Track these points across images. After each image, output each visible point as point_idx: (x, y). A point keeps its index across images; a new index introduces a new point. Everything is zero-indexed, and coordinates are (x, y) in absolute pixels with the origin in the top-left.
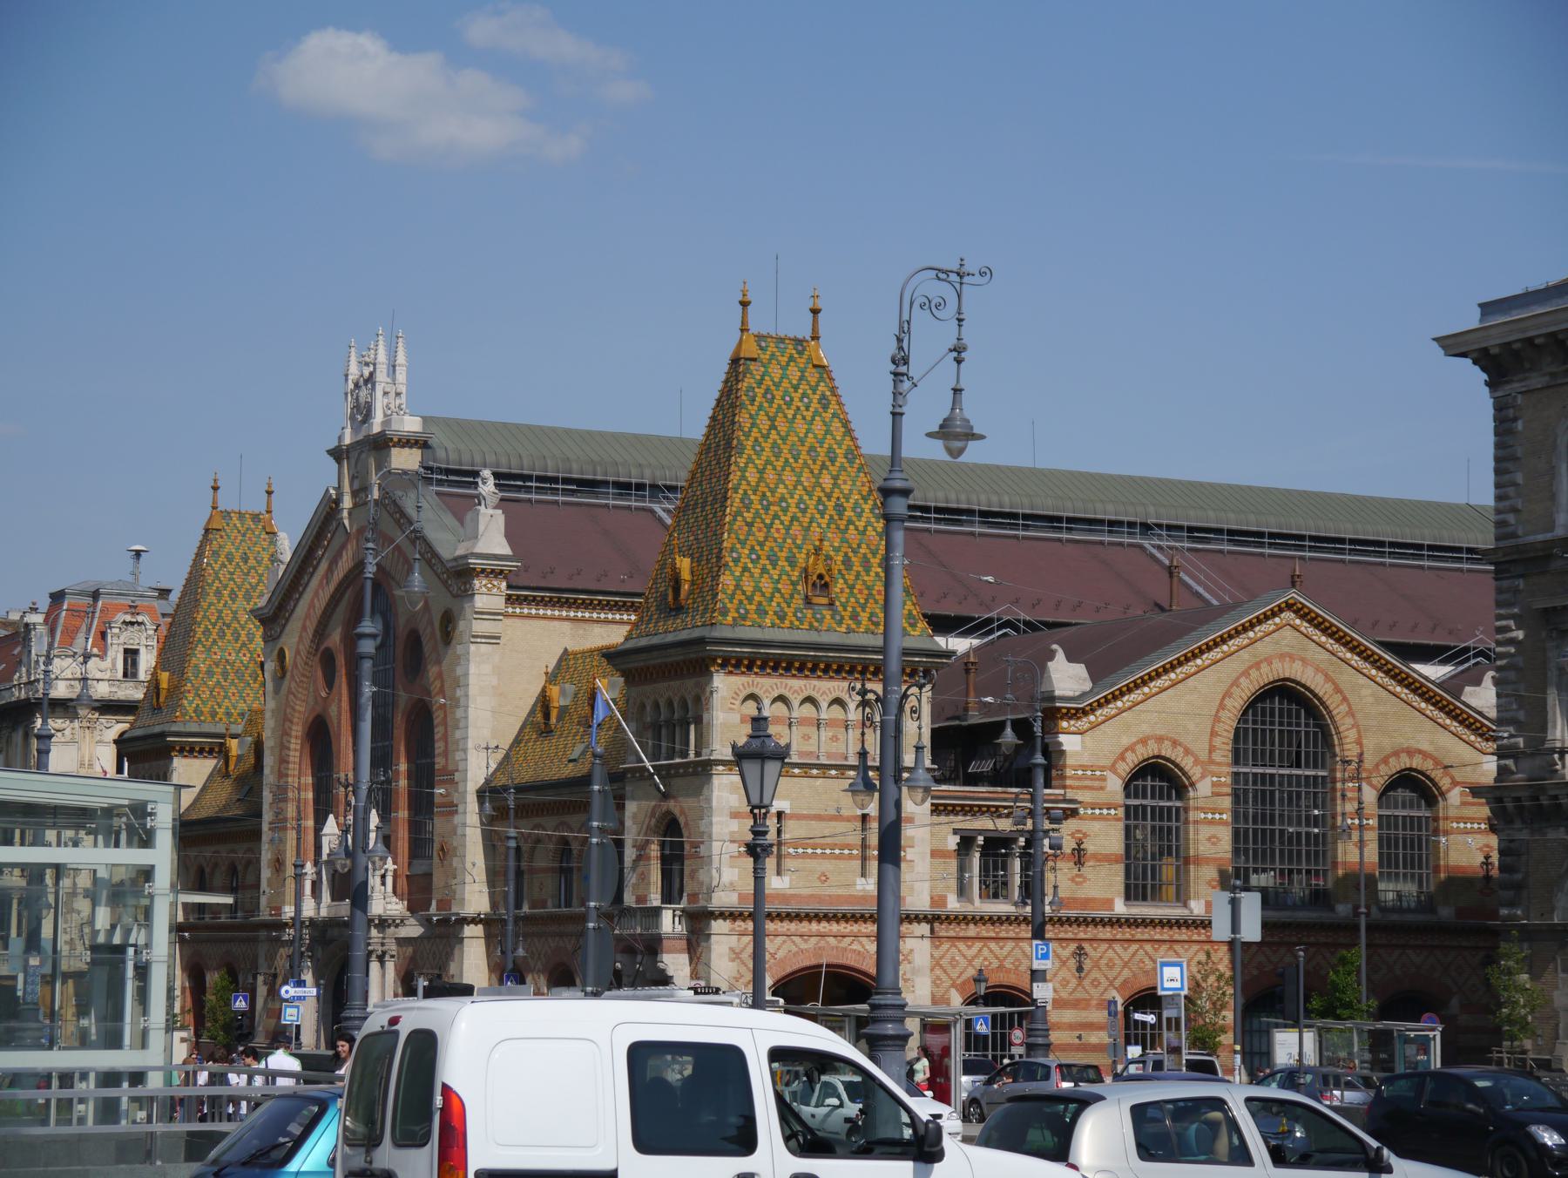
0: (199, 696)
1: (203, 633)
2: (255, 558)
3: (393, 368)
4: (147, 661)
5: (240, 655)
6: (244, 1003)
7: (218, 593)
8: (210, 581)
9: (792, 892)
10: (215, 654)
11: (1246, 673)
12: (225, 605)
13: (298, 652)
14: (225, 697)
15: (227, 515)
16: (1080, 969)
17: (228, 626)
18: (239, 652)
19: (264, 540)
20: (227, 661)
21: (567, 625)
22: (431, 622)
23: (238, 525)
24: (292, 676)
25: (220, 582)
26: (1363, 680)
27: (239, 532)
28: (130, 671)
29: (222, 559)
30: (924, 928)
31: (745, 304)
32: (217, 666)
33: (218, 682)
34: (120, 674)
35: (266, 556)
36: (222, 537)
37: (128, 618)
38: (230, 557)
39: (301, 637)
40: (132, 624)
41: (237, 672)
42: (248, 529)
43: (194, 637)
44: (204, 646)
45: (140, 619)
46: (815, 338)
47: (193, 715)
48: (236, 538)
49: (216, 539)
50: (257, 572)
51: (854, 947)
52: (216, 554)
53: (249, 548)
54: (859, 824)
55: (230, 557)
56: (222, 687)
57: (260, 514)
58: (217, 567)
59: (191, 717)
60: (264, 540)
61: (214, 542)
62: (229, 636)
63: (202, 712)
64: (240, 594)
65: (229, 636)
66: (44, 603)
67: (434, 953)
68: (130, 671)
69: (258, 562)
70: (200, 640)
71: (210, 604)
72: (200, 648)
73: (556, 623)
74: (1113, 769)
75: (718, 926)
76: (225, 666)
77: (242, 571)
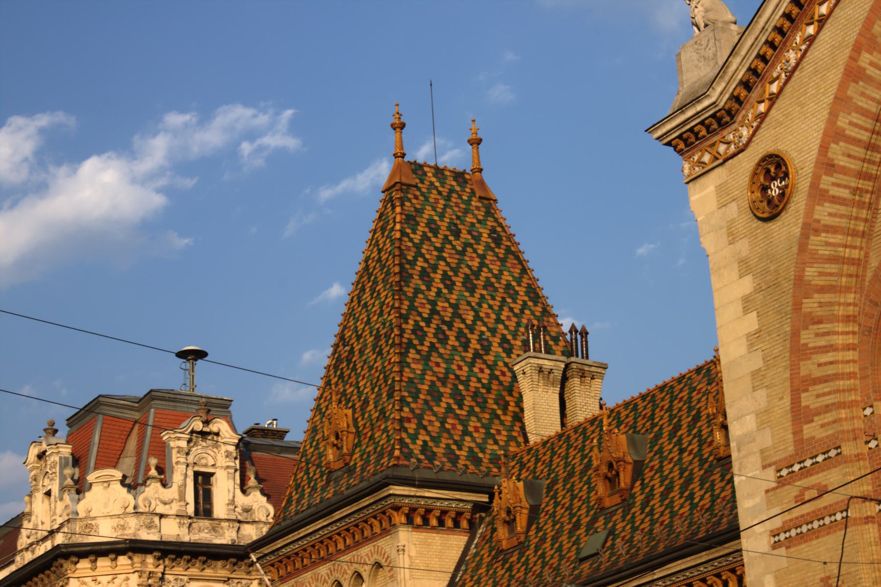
0: (425, 428)
1: (414, 332)
2: (469, 232)
5: (476, 370)
8: (410, 258)
10: (438, 365)
12: (439, 293)
14: (465, 433)
15: (418, 168)
17: (450, 325)
18: (472, 365)
19: (478, 208)
20: (457, 377)
23: (437, 184)
24: (818, 195)
25: (426, 260)
27: (440, 193)
29: (422, 228)
32: (444, 384)
33: (449, 409)
34: (191, 510)
36: (416, 197)
37: (198, 425)
39: (841, 102)
40: (203, 434)
41: (476, 394)
42: (452, 191)
43: (401, 336)
44: (418, 352)
45: (214, 427)
47: (422, 457)
48: (436, 200)
49: (409, 200)
50: (475, 251)
52: (411, 220)
53: (458, 218)
56: (457, 417)
57: (464, 172)
58: (417, 238)
59: (419, 460)
60: (478, 208)
61: (407, 204)
62: (452, 341)
63: (434, 454)
64: (458, 280)
65: (452, 341)
69: (474, 237)
70: (410, 344)
71: (417, 291)
72: (412, 354)
76: (455, 386)
77: (454, 247)
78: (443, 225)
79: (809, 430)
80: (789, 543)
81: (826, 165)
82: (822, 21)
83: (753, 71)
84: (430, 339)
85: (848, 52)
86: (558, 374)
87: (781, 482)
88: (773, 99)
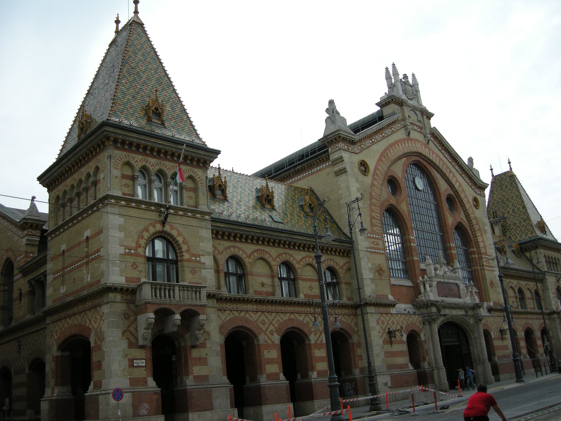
31: (509, 163)
67: (496, 322)
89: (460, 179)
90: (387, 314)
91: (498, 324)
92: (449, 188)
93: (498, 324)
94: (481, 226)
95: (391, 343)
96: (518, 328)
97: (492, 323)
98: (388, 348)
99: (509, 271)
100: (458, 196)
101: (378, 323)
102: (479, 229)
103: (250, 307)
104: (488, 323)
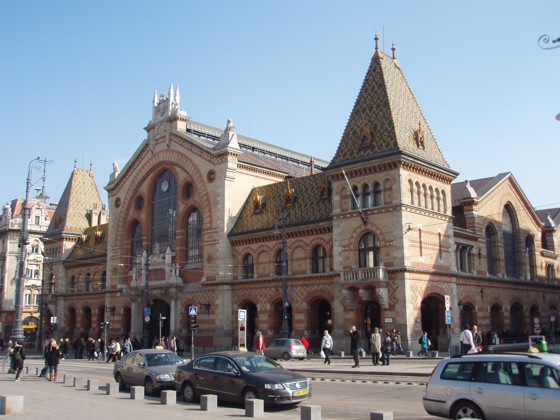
3: (175, 96)
4: (42, 219)
6: (194, 311)
7: (76, 192)
9: (424, 262)
11: (502, 198)
13: (126, 198)
15: (78, 170)
16: (482, 297)
21: (254, 178)
22: (201, 176)
24: (123, 207)
26: (520, 205)
28: (37, 223)
30: (454, 279)
31: (376, 39)
34: (34, 223)
35: (90, 183)
37: (37, 207)
38: (79, 182)
39: (127, 193)
45: (41, 207)
46: (394, 58)
51: (440, 286)
54: (438, 237)
55: (79, 182)
56: (78, 220)
64: (83, 193)
65: (80, 205)
66: (10, 203)
67: (205, 297)
68: (37, 223)
72: (71, 208)
73: (251, 177)
74: (483, 225)
75: (407, 275)
78: (82, 182)
79: (117, 243)
80: (112, 259)
81: (124, 202)
82: (127, 179)
83: (118, 183)
84: (75, 205)
85: (129, 185)
86: (98, 214)
87: (113, 250)
88: (120, 189)
89: (197, 160)
90: (115, 297)
91: (207, 298)
92: (188, 175)
93: (207, 298)
94: (211, 199)
95: (114, 315)
96: (261, 299)
97: (199, 298)
98: (112, 318)
99: (254, 234)
100: (193, 180)
101: (109, 303)
102: (209, 204)
103: (75, 297)
104: (195, 300)
